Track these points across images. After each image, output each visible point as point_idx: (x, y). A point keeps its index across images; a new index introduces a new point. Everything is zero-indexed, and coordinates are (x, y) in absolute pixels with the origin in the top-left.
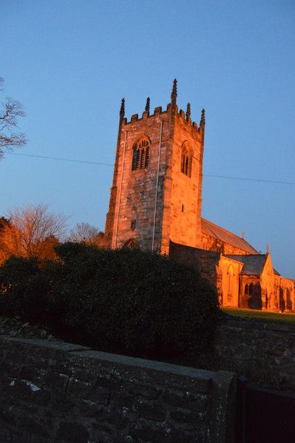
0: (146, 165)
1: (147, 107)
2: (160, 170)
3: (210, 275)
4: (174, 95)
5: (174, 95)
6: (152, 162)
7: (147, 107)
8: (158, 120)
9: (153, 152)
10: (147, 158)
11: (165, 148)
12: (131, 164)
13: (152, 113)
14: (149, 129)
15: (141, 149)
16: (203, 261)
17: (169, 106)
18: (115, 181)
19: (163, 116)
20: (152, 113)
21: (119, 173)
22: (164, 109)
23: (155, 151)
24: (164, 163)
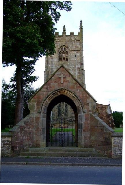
0: (67, 60)
1: (64, 30)
2: (77, 65)
3: (104, 115)
4: (81, 28)
5: (81, 28)
6: (71, 59)
7: (64, 30)
8: (73, 39)
9: (71, 55)
10: (67, 57)
11: (79, 54)
12: (57, 59)
13: (68, 33)
14: (68, 42)
15: (62, 51)
16: (99, 109)
17: (79, 33)
18: (47, 67)
19: (76, 37)
20: (68, 33)
21: (49, 62)
22: (76, 33)
23: (73, 54)
24: (79, 61)
